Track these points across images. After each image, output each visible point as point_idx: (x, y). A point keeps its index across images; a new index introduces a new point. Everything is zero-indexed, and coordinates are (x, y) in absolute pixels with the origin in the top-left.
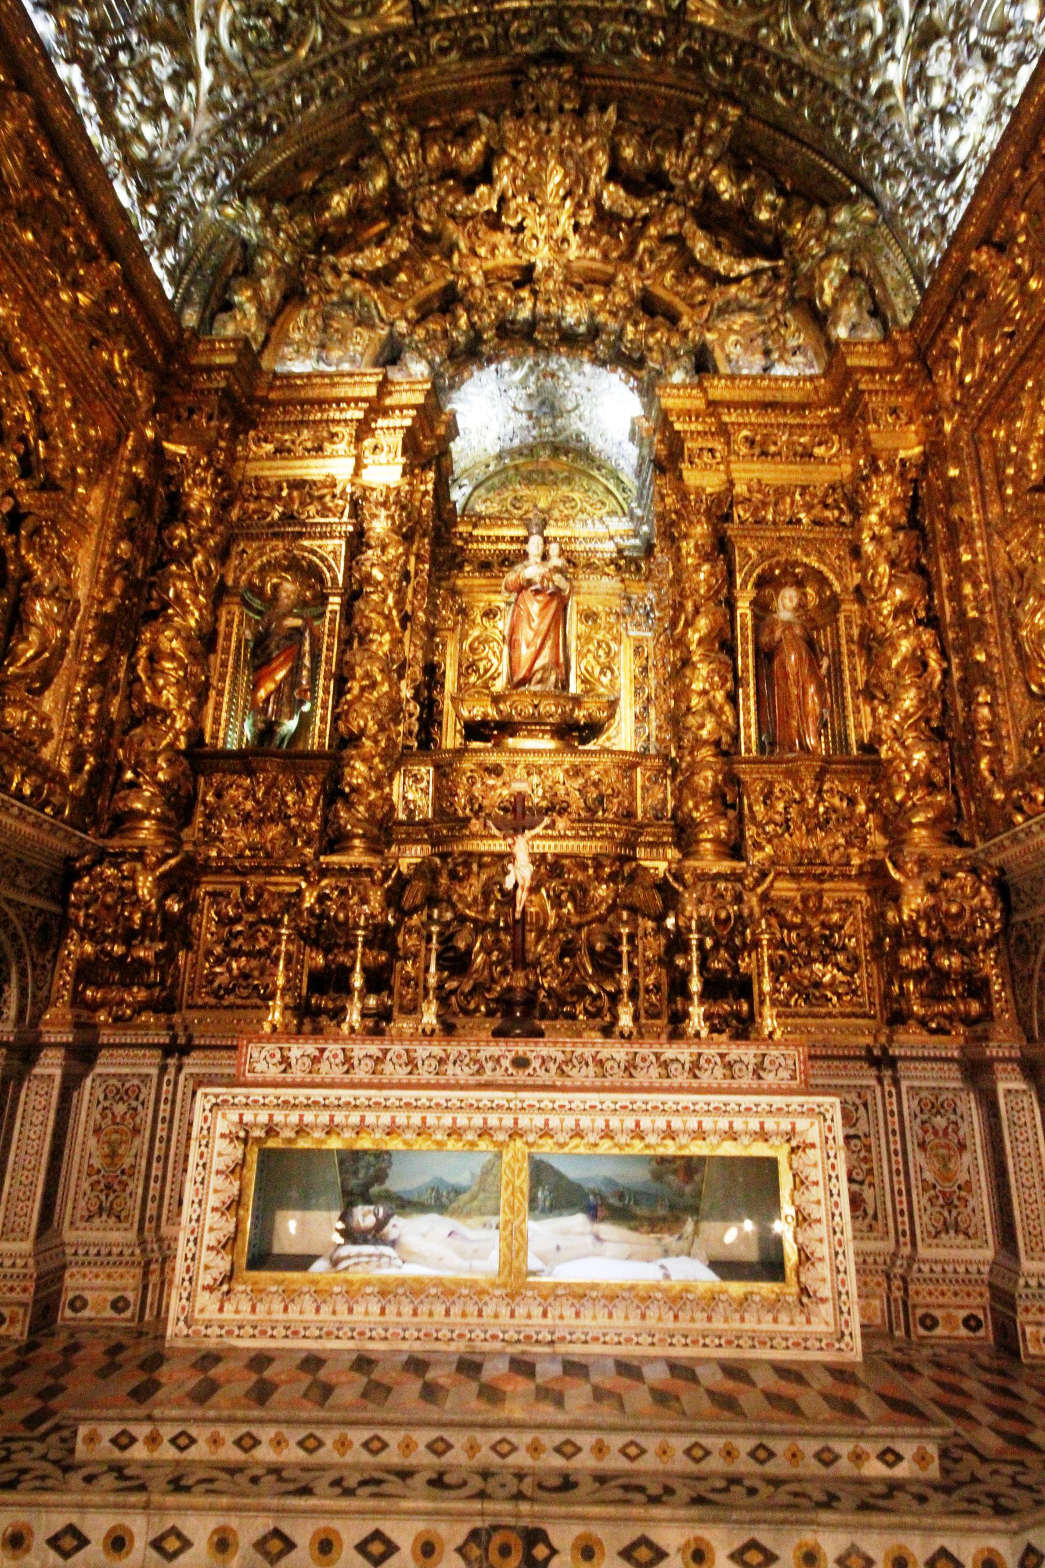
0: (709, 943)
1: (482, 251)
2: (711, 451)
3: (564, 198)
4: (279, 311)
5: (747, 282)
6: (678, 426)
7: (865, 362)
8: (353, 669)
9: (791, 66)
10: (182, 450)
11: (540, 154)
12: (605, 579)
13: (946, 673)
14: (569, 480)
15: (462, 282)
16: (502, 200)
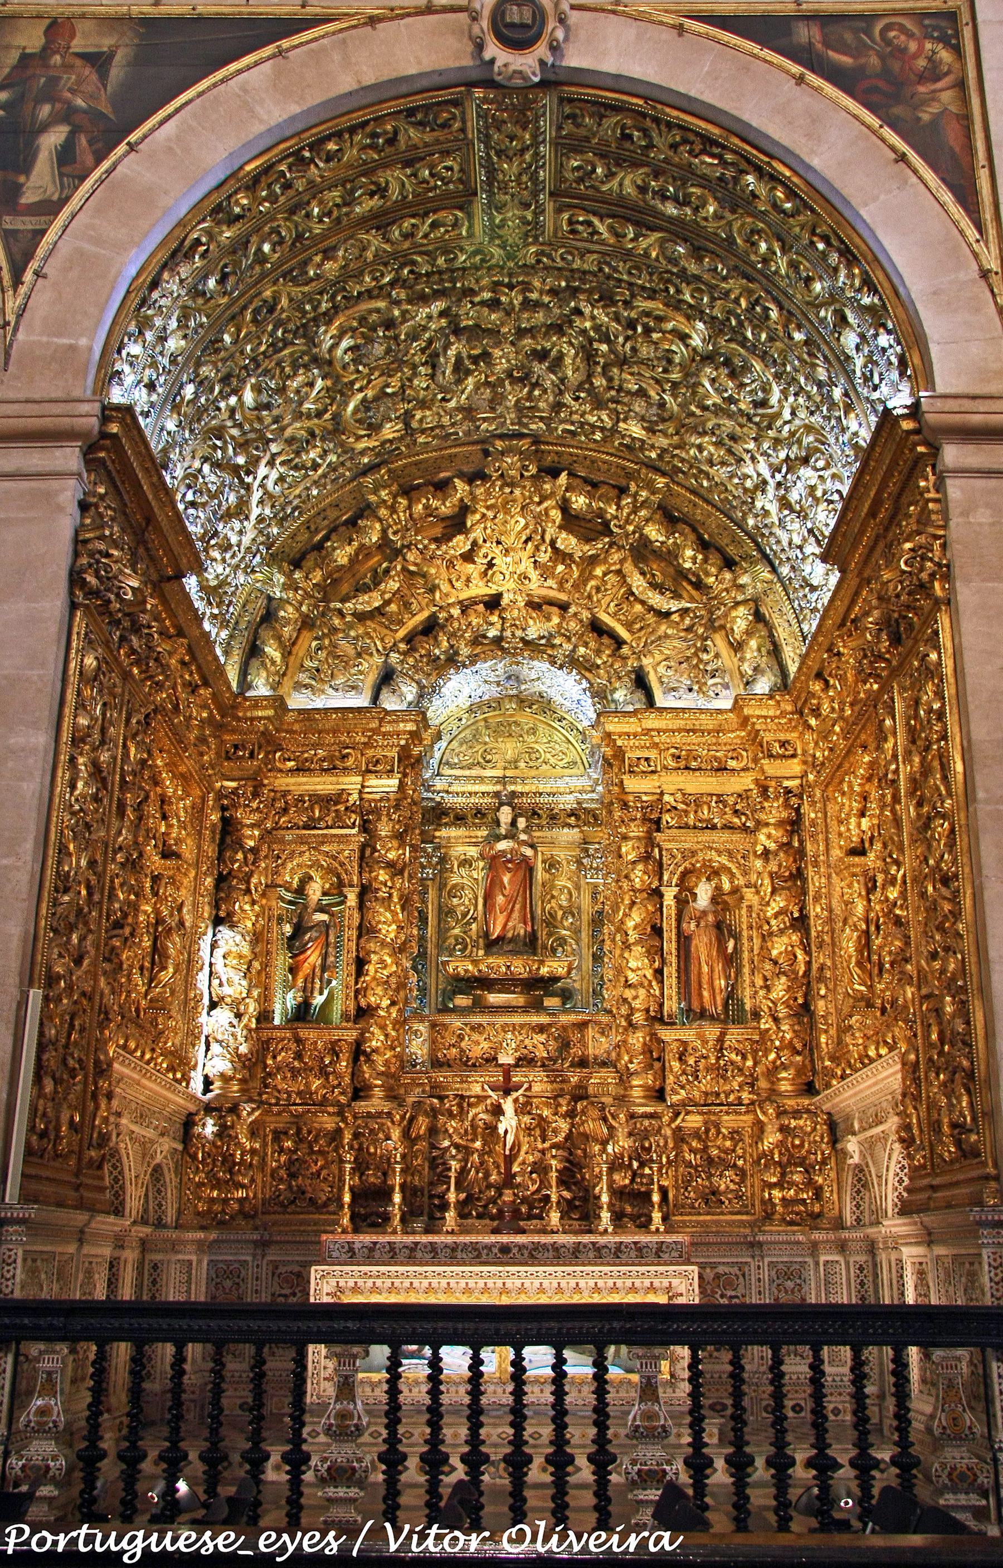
0: (635, 1164)
1: (457, 585)
2: (647, 759)
3: (526, 542)
4: (294, 644)
5: (675, 617)
6: (619, 743)
7: (757, 712)
8: (368, 953)
9: (701, 471)
10: (233, 784)
11: (507, 512)
12: (566, 830)
13: (808, 964)
14: (533, 731)
15: (442, 615)
16: (475, 543)
